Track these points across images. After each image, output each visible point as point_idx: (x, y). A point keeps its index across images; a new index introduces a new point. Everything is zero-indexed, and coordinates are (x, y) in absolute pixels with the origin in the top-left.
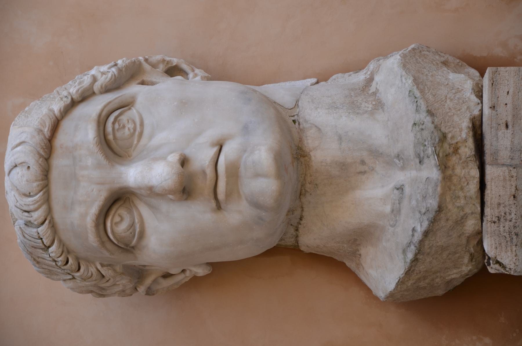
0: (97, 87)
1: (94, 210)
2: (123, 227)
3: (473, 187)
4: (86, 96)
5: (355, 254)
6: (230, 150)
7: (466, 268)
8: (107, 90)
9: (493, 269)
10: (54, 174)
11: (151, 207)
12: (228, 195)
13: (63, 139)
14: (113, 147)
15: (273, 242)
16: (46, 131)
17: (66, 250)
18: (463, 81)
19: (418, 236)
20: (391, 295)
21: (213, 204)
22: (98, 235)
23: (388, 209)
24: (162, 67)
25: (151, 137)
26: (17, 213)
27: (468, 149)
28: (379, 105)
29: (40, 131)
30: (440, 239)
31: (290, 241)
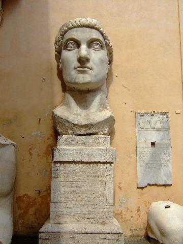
0: (106, 40)
1: (75, 37)
2: (70, 45)
3: (79, 133)
4: (105, 38)
5: (64, 105)
6: (90, 72)
7: (60, 131)
8: (106, 43)
9: (59, 137)
10: (84, 28)
11: (76, 52)
12: (79, 71)
13: (94, 30)
14: (90, 44)
15: (67, 84)
16: (96, 27)
17: (66, 32)
18: (106, 131)
19: (66, 119)
20: (53, 113)
21: (77, 67)
22: (69, 39)
23: (75, 112)
24: (111, 60)
25: (94, 52)
26: (75, 20)
27: (89, 131)
28: (101, 111)
29: (96, 25)
30: (67, 124)
31: (67, 89)
